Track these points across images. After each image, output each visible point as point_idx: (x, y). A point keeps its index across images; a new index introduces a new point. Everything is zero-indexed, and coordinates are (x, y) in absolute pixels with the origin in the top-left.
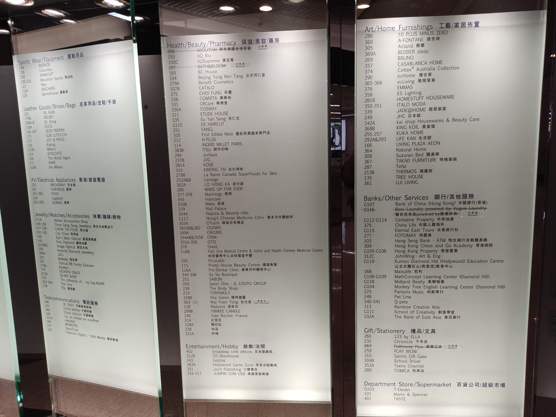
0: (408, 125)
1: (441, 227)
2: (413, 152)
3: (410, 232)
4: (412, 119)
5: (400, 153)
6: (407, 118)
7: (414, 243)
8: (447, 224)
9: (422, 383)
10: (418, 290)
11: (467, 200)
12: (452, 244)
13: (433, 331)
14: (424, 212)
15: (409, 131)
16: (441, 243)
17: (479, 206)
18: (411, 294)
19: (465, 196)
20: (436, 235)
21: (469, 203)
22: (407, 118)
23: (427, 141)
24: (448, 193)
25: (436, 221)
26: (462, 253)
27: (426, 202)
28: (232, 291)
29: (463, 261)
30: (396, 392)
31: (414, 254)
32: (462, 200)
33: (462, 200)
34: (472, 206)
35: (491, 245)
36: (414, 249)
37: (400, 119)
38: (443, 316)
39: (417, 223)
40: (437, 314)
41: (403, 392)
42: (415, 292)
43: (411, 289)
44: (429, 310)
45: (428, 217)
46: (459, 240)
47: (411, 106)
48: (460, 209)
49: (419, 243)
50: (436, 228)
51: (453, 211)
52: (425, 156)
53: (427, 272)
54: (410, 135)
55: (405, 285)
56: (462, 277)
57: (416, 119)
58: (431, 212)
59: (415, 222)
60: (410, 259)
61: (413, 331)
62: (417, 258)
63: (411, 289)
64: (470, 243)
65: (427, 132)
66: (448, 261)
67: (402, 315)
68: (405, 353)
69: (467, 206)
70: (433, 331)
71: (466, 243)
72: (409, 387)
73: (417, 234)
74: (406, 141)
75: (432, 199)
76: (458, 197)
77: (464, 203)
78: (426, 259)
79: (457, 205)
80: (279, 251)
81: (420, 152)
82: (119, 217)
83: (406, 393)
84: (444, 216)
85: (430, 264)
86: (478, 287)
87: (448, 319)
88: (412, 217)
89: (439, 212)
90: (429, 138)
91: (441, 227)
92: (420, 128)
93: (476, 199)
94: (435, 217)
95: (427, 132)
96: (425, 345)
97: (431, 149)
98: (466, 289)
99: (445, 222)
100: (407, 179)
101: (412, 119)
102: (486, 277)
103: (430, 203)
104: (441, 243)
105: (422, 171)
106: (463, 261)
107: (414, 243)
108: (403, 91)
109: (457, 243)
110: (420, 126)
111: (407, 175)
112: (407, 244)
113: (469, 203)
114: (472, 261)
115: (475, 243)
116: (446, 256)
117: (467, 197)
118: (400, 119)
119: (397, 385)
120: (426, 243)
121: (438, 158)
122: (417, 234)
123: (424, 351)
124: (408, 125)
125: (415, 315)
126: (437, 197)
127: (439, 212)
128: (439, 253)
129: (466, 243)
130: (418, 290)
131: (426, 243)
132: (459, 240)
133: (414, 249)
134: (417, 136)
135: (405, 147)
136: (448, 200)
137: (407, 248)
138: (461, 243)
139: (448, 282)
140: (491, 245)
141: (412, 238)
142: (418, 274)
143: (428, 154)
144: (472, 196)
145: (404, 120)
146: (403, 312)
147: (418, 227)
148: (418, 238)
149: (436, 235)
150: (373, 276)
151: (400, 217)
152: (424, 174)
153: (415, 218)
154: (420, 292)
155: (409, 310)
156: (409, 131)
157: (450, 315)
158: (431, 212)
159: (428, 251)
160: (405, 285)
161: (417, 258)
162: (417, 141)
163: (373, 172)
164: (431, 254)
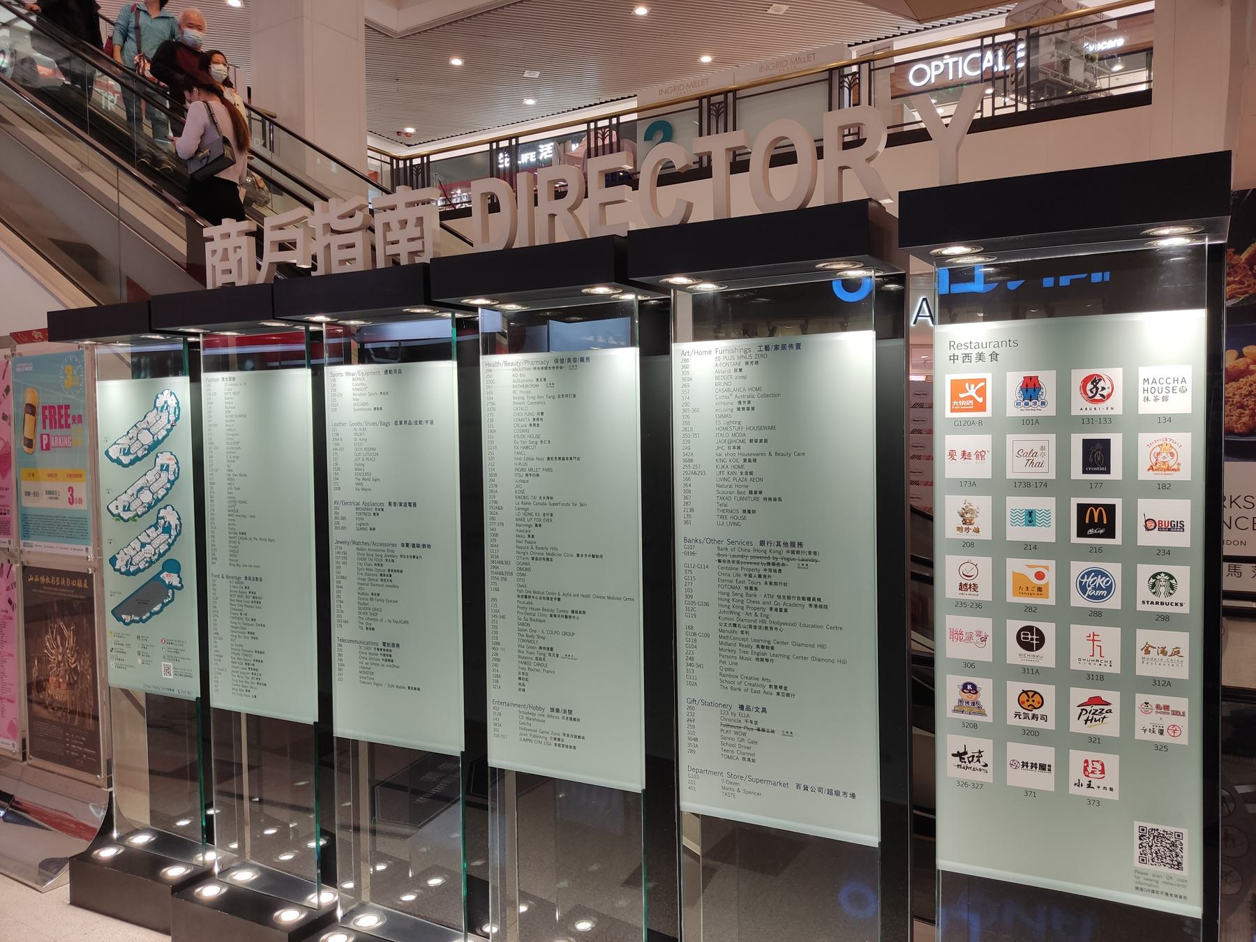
0: (729, 457)
1: (768, 580)
2: (735, 490)
3: (734, 584)
4: (732, 451)
5: (721, 490)
6: (727, 450)
7: (738, 597)
8: (775, 577)
9: (753, 777)
10: (745, 656)
11: (796, 549)
12: (781, 601)
13: (764, 710)
14: (749, 560)
15: (730, 464)
16: (768, 600)
17: (810, 557)
18: (738, 660)
19: (793, 544)
20: (763, 589)
21: (798, 552)
22: (727, 450)
23: (749, 477)
24: (774, 539)
25: (762, 573)
26: (794, 614)
27: (751, 548)
28: (540, 640)
29: (794, 624)
30: (724, 784)
31: (739, 610)
32: (790, 549)
33: (790, 549)
34: (801, 556)
35: (826, 607)
36: (739, 604)
37: (720, 451)
38: (774, 691)
39: (742, 573)
40: (767, 689)
41: (733, 786)
42: (742, 658)
43: (738, 654)
44: (760, 682)
45: (753, 566)
46: (789, 597)
47: (730, 437)
48: (788, 559)
49: (745, 598)
50: (762, 580)
51: (781, 562)
52: (747, 494)
53: (754, 634)
54: (730, 470)
55: (731, 648)
56: (795, 644)
57: (736, 451)
58: (756, 561)
59: (739, 572)
60: (735, 616)
61: (742, 707)
62: (743, 616)
63: (738, 654)
64: (801, 602)
65: (748, 467)
66: (778, 623)
67: (729, 686)
68: (732, 735)
69: (796, 556)
70: (764, 710)
71: (796, 602)
72: (738, 780)
73: (743, 586)
74: (726, 476)
75: (757, 545)
76: (786, 544)
77: (793, 552)
78: (753, 618)
79: (787, 556)
80: (588, 596)
81: (742, 490)
82: (429, 546)
83: (736, 787)
84: (773, 568)
85: (758, 624)
86: (814, 659)
87: (780, 697)
88: (735, 565)
89: (765, 561)
90: (751, 473)
91: (768, 580)
92: (742, 463)
93: (805, 548)
94: (761, 567)
95: (748, 467)
96: (755, 727)
97: (753, 486)
98: (800, 660)
99: (772, 574)
100: (729, 520)
101: (732, 451)
102: (822, 646)
103: (755, 550)
104: (768, 600)
105: (744, 511)
106: (794, 624)
107: (738, 597)
108: (722, 420)
109: (787, 601)
110: (741, 459)
111: (729, 515)
112: (731, 597)
113: (798, 552)
114: (804, 625)
115: (807, 603)
116: (775, 616)
117: (796, 546)
118: (720, 451)
119: (725, 775)
120: (753, 599)
121: (761, 497)
122: (743, 586)
123: (753, 735)
124: (729, 457)
125: (743, 687)
126: (762, 543)
127: (765, 561)
128: (767, 612)
129: (796, 602)
130: (745, 656)
131: (753, 599)
132: (789, 597)
133: (739, 604)
134: (738, 471)
135: (726, 483)
136: (775, 548)
137: (731, 603)
138: (791, 601)
139: (779, 649)
140: (826, 607)
141: (736, 591)
142: (745, 636)
143: (751, 492)
144: (800, 544)
145: (724, 453)
146: (729, 682)
147: (742, 578)
148: (743, 591)
149: (763, 589)
150: (695, 634)
151: (722, 564)
152: (747, 514)
153: (739, 566)
154: (748, 659)
155: (737, 680)
156: (730, 464)
157: (782, 691)
158: (756, 561)
159: (754, 609)
160: (731, 648)
161: (743, 616)
162: (738, 476)
163: (692, 510)
164: (759, 613)
